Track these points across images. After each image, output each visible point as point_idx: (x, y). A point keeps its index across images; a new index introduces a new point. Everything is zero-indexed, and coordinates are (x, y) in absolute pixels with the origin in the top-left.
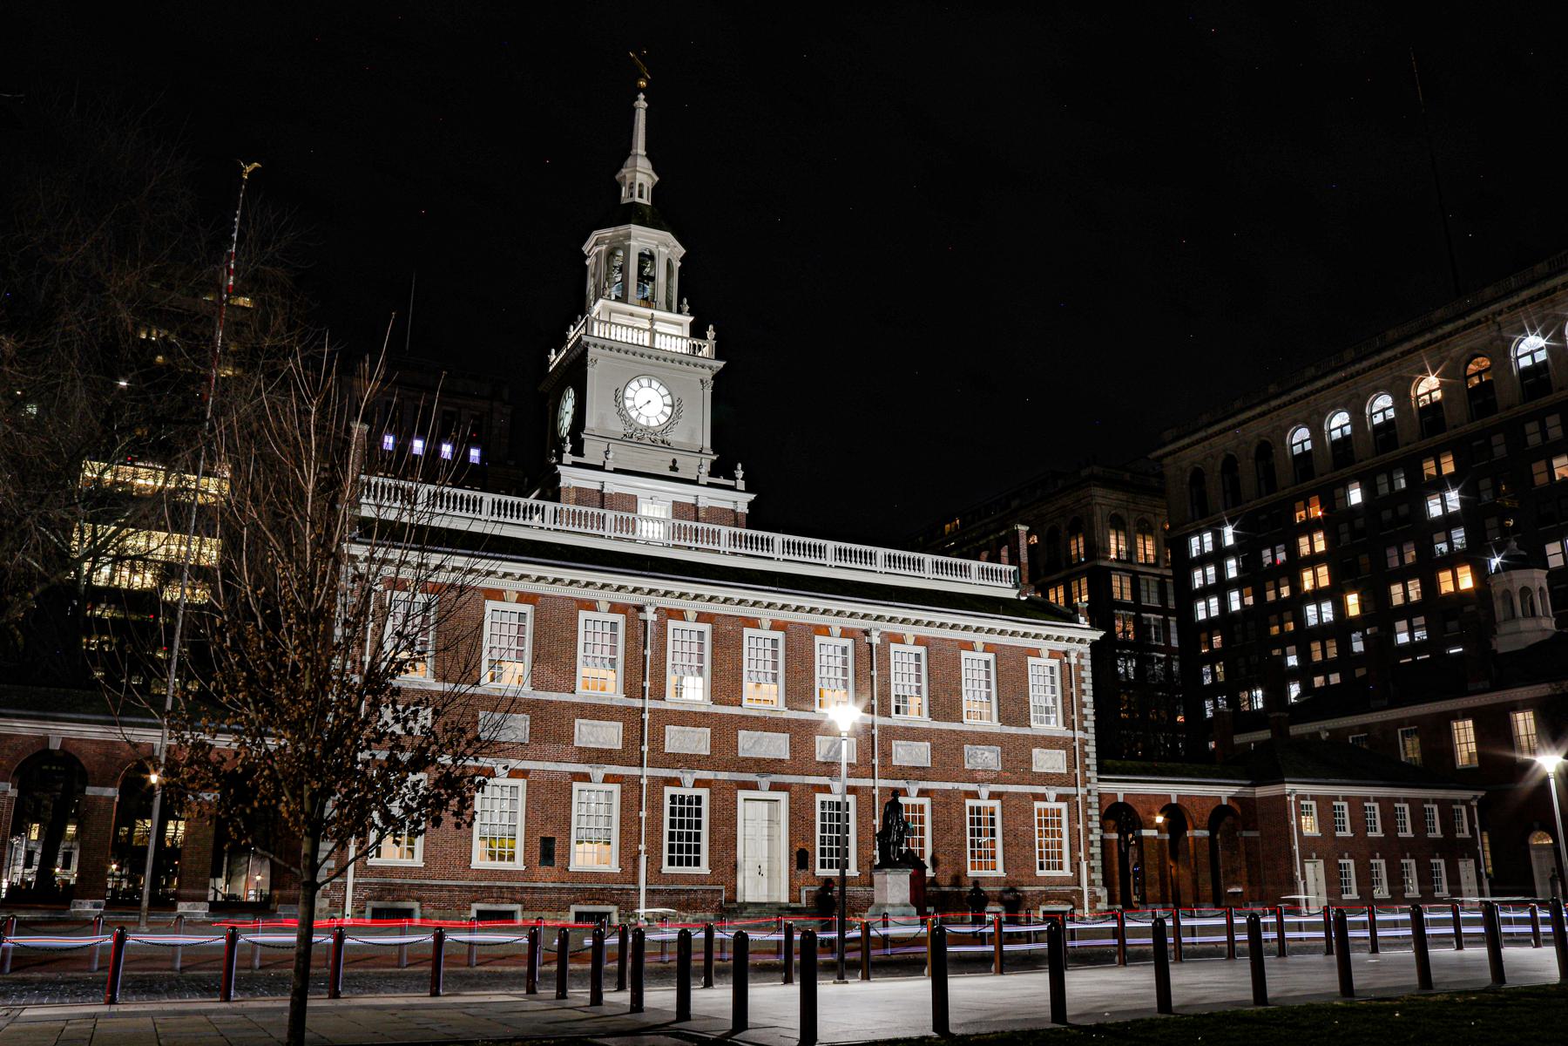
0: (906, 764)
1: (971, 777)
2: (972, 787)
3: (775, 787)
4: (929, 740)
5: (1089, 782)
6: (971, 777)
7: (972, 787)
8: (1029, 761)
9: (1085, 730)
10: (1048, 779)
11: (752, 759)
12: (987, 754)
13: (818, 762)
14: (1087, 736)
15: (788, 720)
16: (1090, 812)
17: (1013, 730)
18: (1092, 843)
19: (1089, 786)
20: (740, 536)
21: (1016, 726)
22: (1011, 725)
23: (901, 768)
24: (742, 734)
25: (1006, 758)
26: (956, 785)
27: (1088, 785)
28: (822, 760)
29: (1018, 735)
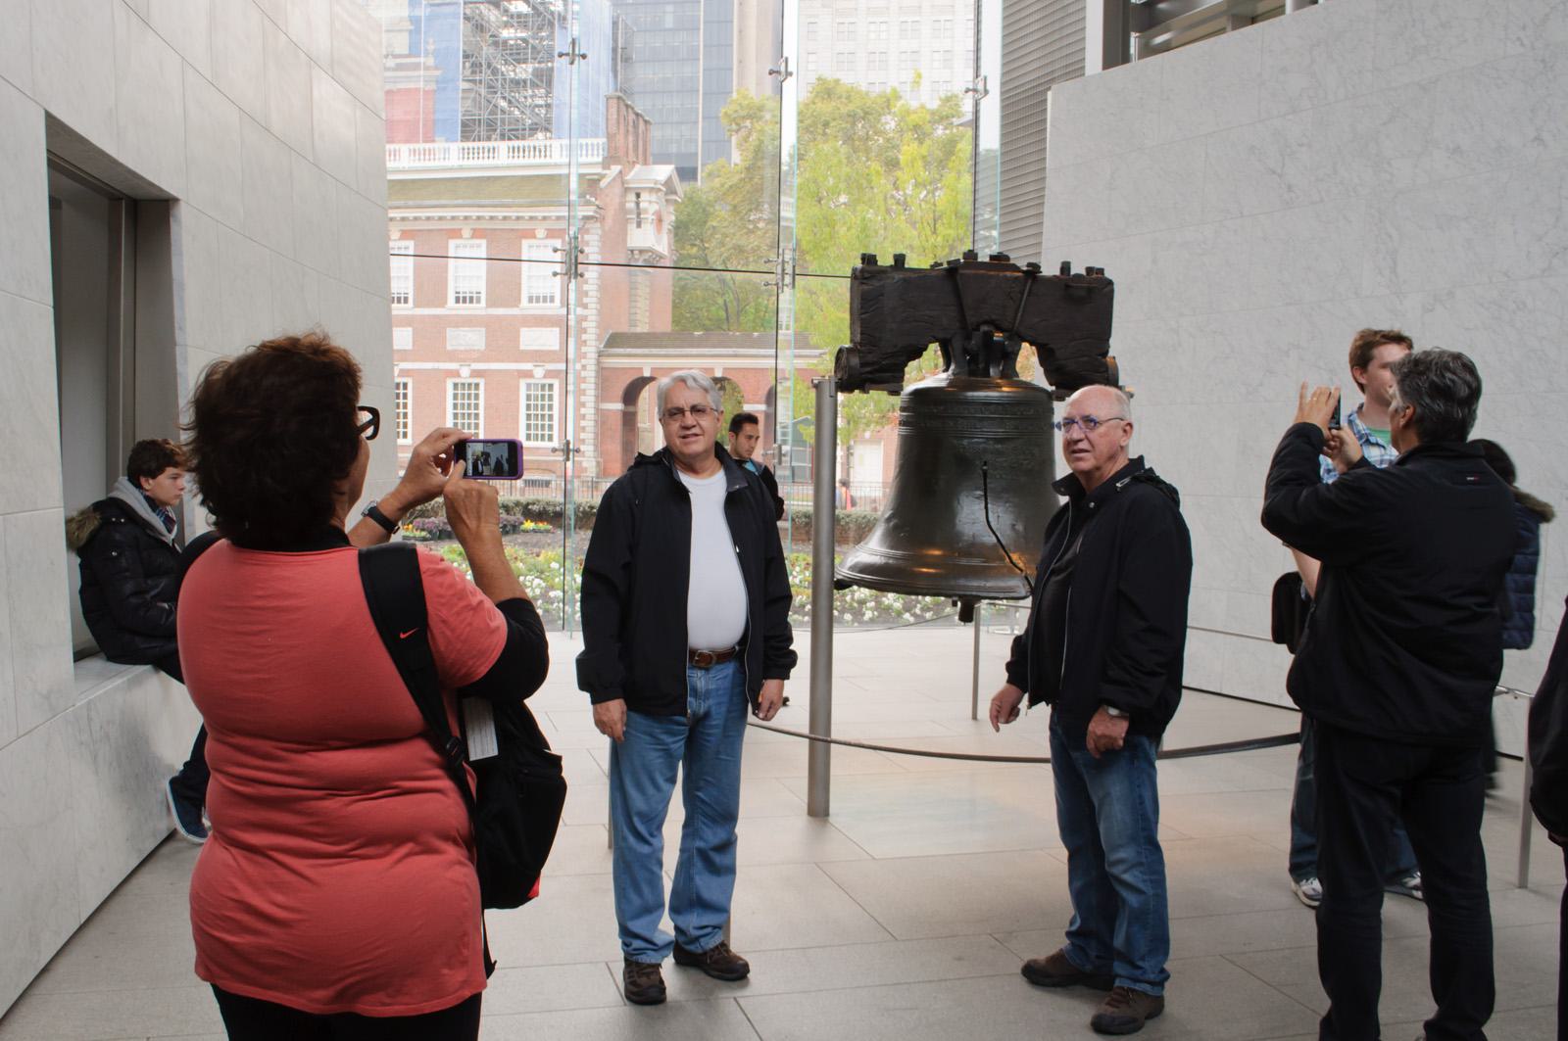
1: (452, 356)
2: (453, 366)
4: (409, 325)
5: (585, 358)
6: (452, 356)
7: (453, 366)
8: (516, 339)
9: (585, 307)
10: (539, 356)
14: (585, 312)
16: (583, 386)
17: (500, 311)
18: (583, 417)
19: (583, 361)
20: (592, 145)
26: (436, 365)
27: (583, 360)
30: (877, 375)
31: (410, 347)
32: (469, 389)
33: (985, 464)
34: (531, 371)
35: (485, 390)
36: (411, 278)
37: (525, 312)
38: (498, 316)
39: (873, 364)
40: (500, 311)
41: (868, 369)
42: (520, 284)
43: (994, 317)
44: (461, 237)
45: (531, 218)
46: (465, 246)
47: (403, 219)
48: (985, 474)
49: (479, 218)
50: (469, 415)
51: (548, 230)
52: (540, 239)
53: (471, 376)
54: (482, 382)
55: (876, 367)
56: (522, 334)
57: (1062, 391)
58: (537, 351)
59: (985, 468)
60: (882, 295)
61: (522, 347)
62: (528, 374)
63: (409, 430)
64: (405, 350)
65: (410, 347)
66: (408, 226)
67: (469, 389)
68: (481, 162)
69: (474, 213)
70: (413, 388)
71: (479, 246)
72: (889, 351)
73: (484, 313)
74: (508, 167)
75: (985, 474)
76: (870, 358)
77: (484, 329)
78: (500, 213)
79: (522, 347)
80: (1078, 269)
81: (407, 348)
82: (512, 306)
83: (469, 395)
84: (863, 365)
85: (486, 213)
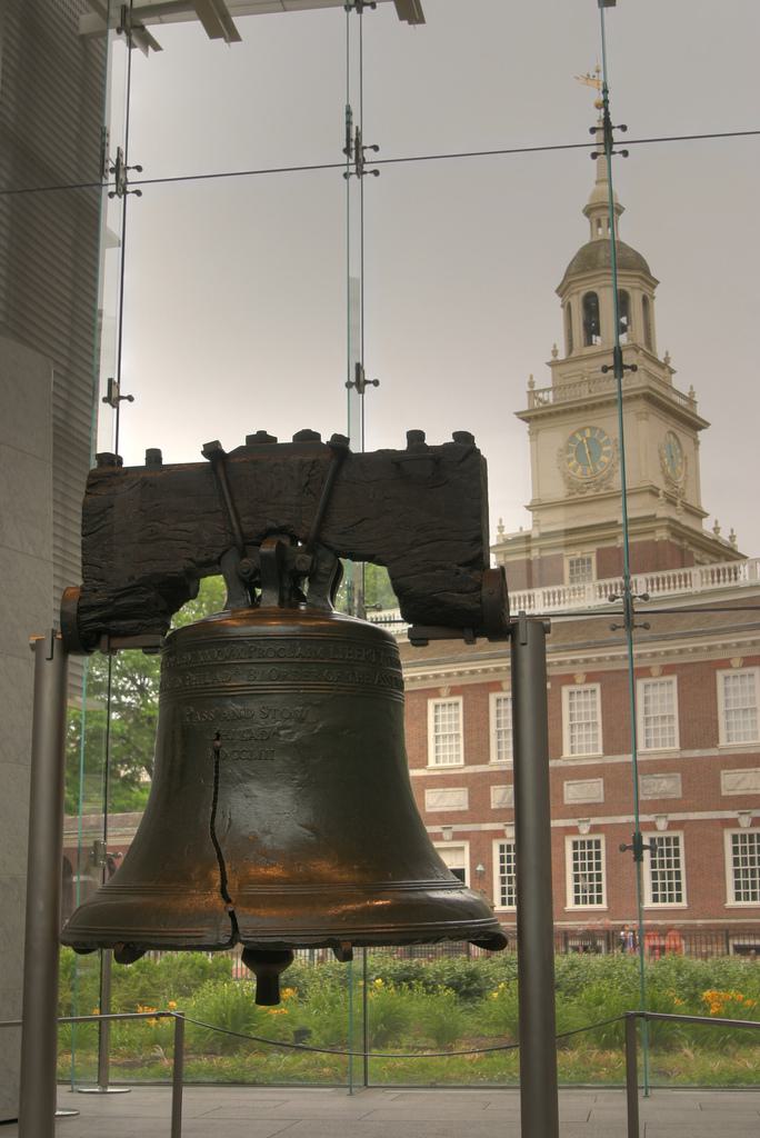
0: (577, 802)
3: (458, 836)
11: (437, 813)
12: (665, 782)
13: (495, 810)
15: (466, 775)
17: (696, 753)
21: (701, 747)
22: (694, 748)
23: (573, 807)
24: (427, 791)
25: (687, 783)
28: (497, 807)
29: (702, 758)
30: (114, 623)
31: (602, 800)
32: (668, 844)
33: (218, 737)
34: (736, 819)
35: (685, 843)
36: (600, 724)
37: (725, 753)
38: (694, 759)
39: (101, 606)
40: (696, 753)
41: (94, 615)
42: (717, 721)
43: (283, 522)
44: (650, 676)
45: (725, 646)
46: (655, 685)
47: (587, 661)
48: (217, 753)
49: (667, 653)
50: (670, 873)
51: (744, 658)
52: (737, 668)
53: (669, 828)
54: (680, 834)
55: (109, 610)
56: (722, 777)
57: (424, 631)
58: (740, 796)
59: (218, 743)
60: (112, 507)
61: (724, 793)
62: (734, 823)
63: (604, 894)
64: (596, 804)
65: (602, 800)
66: (593, 668)
67: (668, 844)
68: (672, 592)
69: (661, 647)
70: (606, 845)
71: (670, 683)
72: (123, 586)
73: (678, 757)
74: (703, 594)
75: (217, 753)
76: (95, 599)
77: (679, 775)
78: (689, 644)
79: (724, 793)
80: (437, 437)
81: (598, 801)
82: (708, 747)
83: (668, 850)
84: (81, 610)
85: (674, 646)
